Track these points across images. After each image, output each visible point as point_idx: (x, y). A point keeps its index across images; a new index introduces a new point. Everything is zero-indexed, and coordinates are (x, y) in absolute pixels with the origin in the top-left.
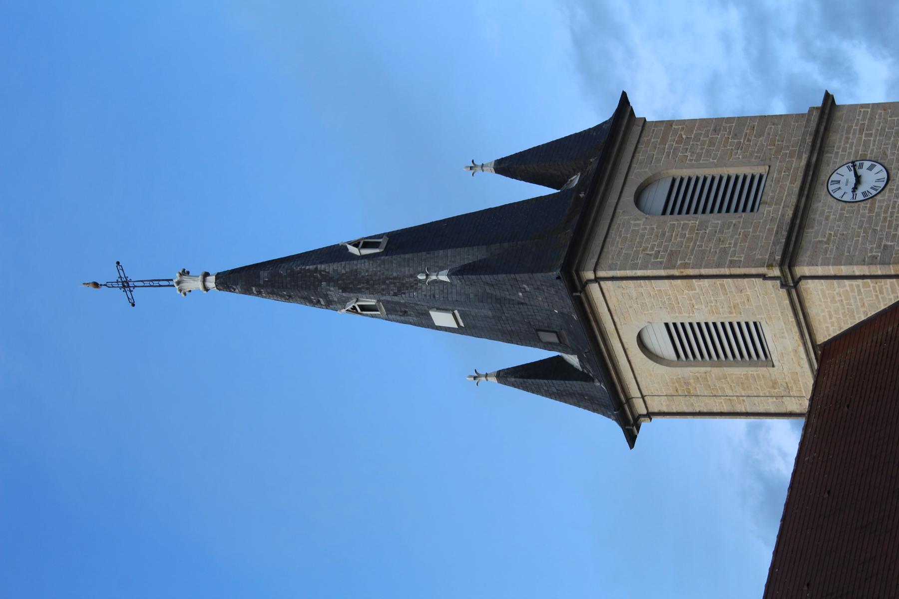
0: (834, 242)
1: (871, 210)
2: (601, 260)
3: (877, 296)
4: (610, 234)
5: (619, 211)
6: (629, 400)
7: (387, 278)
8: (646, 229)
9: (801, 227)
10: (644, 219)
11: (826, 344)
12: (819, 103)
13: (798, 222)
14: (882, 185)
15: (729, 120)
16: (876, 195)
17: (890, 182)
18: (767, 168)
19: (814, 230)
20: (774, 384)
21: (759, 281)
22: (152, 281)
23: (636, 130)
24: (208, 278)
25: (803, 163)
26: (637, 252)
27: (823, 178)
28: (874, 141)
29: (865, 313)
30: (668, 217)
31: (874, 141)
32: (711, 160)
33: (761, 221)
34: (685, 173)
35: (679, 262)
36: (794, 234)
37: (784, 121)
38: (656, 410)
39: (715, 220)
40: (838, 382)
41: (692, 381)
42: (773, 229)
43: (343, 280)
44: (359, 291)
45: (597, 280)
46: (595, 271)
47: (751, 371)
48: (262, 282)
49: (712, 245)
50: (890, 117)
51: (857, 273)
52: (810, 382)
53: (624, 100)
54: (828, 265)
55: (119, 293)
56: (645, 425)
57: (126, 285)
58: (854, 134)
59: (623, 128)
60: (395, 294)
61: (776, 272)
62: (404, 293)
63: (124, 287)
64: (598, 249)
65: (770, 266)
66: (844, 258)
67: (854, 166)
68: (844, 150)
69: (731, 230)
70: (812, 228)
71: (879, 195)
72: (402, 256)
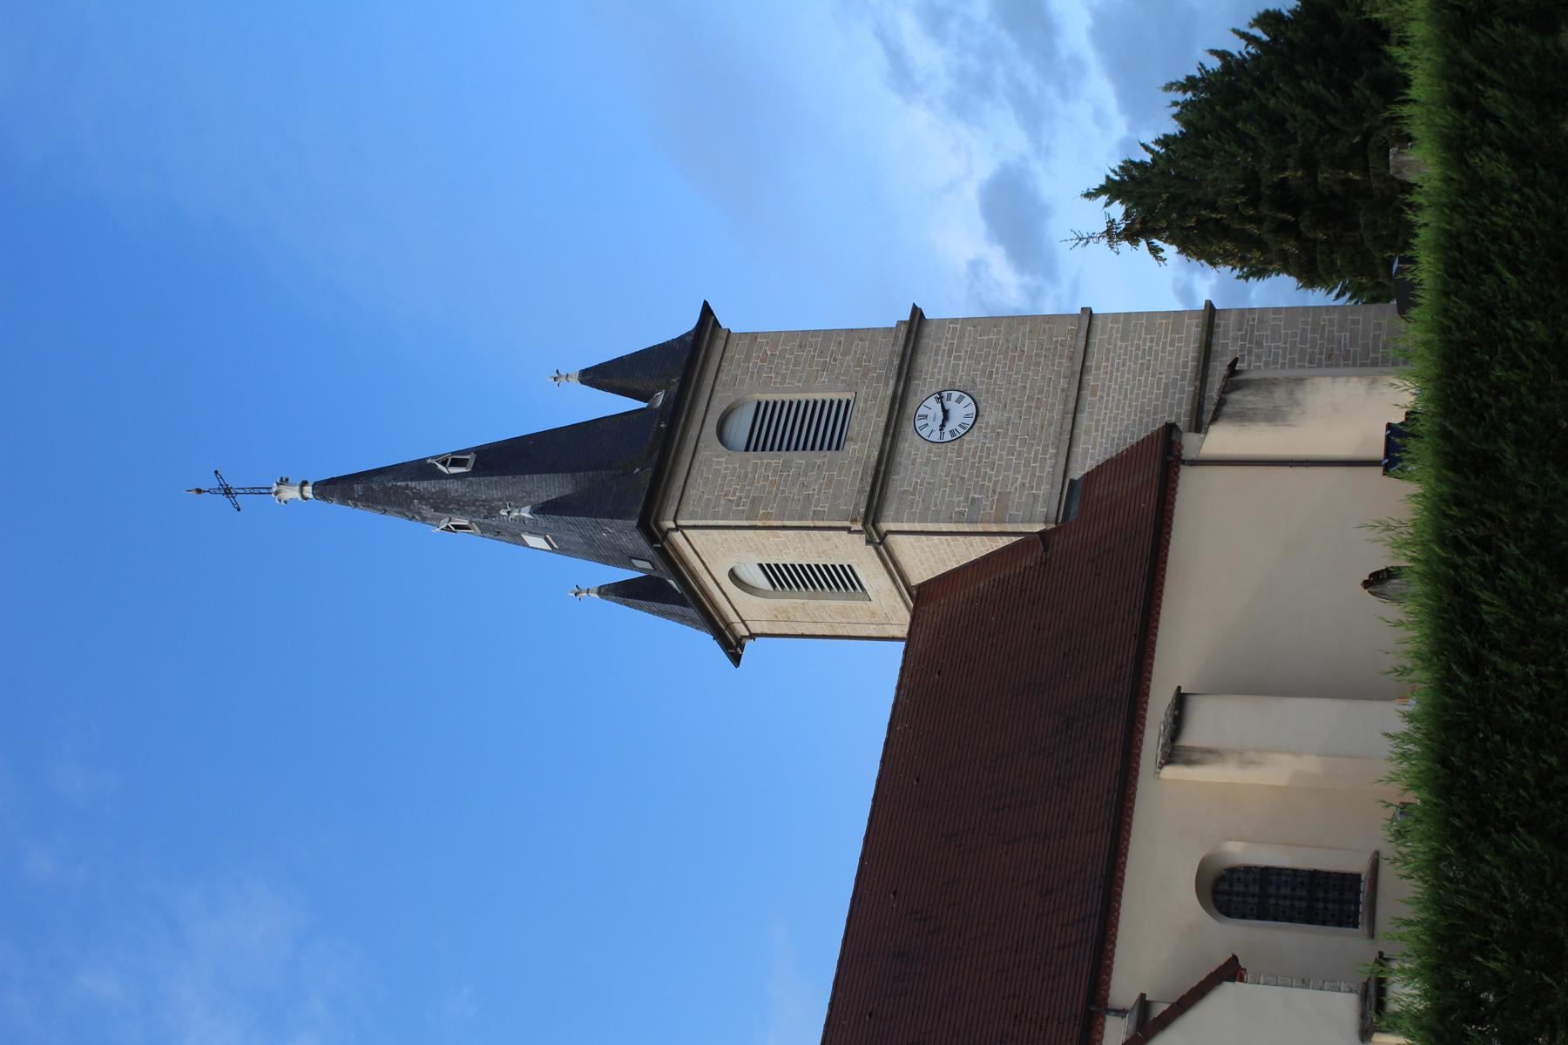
0: (920, 494)
1: (959, 454)
2: (681, 507)
3: (967, 549)
4: (691, 474)
5: (701, 444)
6: (729, 625)
7: (477, 500)
8: (727, 468)
9: (887, 473)
10: (727, 456)
11: (920, 586)
12: (907, 318)
13: (883, 468)
14: (970, 421)
15: (815, 333)
16: (964, 435)
17: (979, 418)
18: (854, 394)
19: (899, 477)
20: (873, 614)
21: (845, 533)
22: (252, 488)
23: (720, 343)
24: (305, 488)
25: (890, 392)
26: (718, 497)
27: (910, 411)
28: (963, 366)
29: (957, 562)
30: (751, 454)
31: (963, 366)
32: (796, 384)
33: (846, 462)
34: (771, 397)
35: (761, 512)
36: (879, 484)
37: (872, 336)
38: (759, 632)
39: (799, 459)
40: (931, 638)
41: (790, 610)
42: (858, 471)
43: (434, 499)
44: (449, 511)
45: (678, 528)
46: (675, 521)
47: (848, 603)
48: (356, 496)
49: (795, 491)
50: (980, 336)
51: (944, 530)
52: (906, 617)
53: (707, 311)
54: (914, 522)
55: (232, 483)
56: (749, 644)
57: (227, 491)
58: (943, 356)
59: (705, 344)
60: (486, 517)
61: (858, 526)
62: (494, 517)
63: (226, 493)
64: (678, 494)
65: (854, 521)
66: (930, 513)
67: (941, 398)
68: (932, 376)
69: (815, 473)
70: (898, 474)
71: (967, 435)
72: (489, 478)
